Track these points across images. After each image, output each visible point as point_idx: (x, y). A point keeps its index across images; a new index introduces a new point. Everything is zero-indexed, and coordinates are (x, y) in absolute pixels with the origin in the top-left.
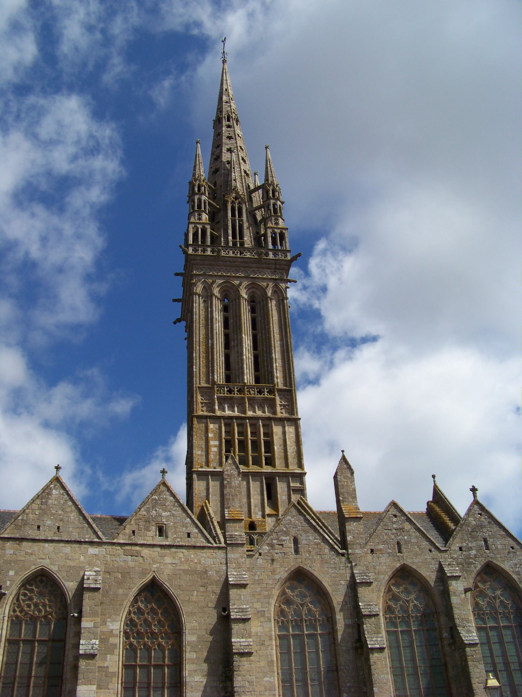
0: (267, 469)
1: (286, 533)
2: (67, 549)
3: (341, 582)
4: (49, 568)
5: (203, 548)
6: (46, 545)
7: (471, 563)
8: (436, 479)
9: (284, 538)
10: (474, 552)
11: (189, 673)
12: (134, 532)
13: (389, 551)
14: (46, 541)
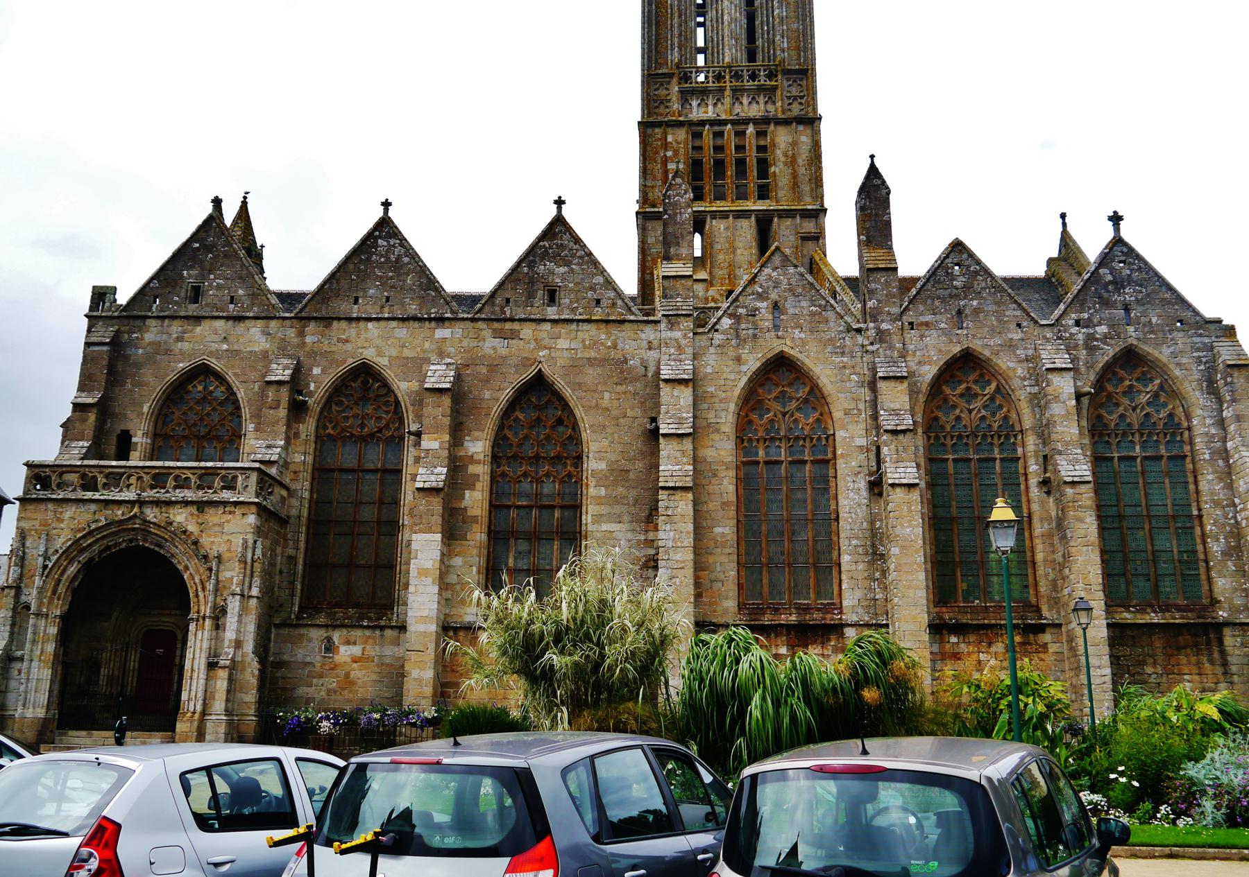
0: (761, 206)
1: (761, 297)
2: (401, 332)
4: (374, 360)
5: (623, 322)
6: (370, 325)
7: (1097, 348)
8: (1067, 220)
9: (759, 304)
10: (1103, 329)
12: (508, 301)
13: (943, 325)
14: (370, 319)
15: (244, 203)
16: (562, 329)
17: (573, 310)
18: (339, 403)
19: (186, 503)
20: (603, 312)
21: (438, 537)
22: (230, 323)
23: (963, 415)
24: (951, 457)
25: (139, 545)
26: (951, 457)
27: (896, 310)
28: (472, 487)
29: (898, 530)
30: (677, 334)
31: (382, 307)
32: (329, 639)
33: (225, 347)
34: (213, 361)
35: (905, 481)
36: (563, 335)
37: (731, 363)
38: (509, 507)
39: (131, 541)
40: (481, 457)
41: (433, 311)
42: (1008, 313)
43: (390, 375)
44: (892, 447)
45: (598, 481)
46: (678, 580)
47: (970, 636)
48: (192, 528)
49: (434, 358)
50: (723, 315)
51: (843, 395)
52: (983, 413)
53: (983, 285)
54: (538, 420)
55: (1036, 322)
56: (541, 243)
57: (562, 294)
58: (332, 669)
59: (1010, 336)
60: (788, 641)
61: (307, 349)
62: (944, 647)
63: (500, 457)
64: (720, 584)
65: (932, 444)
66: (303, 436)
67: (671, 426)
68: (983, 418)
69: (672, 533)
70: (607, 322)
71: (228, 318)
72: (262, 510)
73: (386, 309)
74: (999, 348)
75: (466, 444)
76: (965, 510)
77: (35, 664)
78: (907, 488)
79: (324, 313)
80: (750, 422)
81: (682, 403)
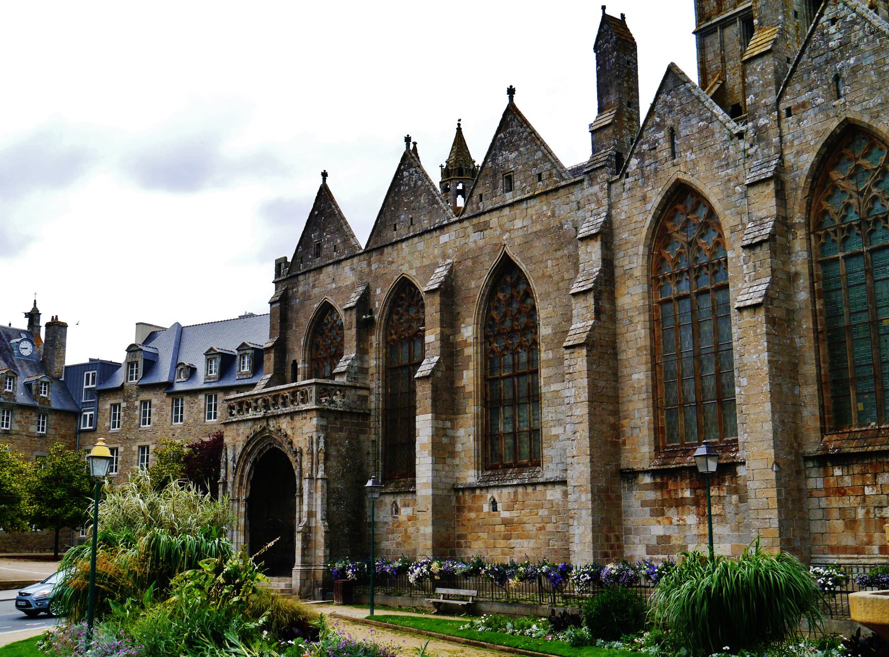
1: (659, 127)
2: (420, 244)
3: (737, 188)
5: (556, 190)
6: (404, 245)
11: (544, 381)
12: (481, 195)
13: (820, 101)
14: (402, 241)
15: (459, 130)
16: (517, 210)
17: (523, 190)
18: (398, 313)
19: (286, 415)
20: (543, 184)
21: (429, 416)
22: (335, 266)
23: (852, 201)
24: (840, 255)
25: (274, 447)
26: (840, 255)
27: (771, 99)
28: (468, 369)
29: (746, 359)
30: (596, 188)
31: (409, 228)
32: (395, 502)
33: (334, 285)
34: (329, 298)
35: (749, 303)
36: (518, 216)
37: (638, 204)
38: (497, 379)
39: (270, 444)
40: (471, 340)
41: (437, 221)
43: (416, 282)
44: (751, 263)
45: (546, 345)
46: (578, 434)
47: (855, 467)
48: (289, 432)
49: (440, 261)
50: (630, 157)
51: (728, 212)
52: (875, 191)
53: (861, 34)
54: (512, 296)
56: (499, 136)
58: (398, 527)
60: (691, 483)
61: (373, 275)
62: (828, 481)
63: (490, 336)
64: (638, 430)
65: (823, 245)
66: (374, 345)
67: (581, 284)
68: (875, 199)
69: (573, 390)
70: (546, 193)
71: (333, 263)
72: (322, 413)
73: (411, 229)
74: (879, 108)
75: (463, 330)
76: (859, 315)
77: (235, 533)
78: (752, 311)
79: (380, 245)
80: (663, 260)
81: (593, 259)
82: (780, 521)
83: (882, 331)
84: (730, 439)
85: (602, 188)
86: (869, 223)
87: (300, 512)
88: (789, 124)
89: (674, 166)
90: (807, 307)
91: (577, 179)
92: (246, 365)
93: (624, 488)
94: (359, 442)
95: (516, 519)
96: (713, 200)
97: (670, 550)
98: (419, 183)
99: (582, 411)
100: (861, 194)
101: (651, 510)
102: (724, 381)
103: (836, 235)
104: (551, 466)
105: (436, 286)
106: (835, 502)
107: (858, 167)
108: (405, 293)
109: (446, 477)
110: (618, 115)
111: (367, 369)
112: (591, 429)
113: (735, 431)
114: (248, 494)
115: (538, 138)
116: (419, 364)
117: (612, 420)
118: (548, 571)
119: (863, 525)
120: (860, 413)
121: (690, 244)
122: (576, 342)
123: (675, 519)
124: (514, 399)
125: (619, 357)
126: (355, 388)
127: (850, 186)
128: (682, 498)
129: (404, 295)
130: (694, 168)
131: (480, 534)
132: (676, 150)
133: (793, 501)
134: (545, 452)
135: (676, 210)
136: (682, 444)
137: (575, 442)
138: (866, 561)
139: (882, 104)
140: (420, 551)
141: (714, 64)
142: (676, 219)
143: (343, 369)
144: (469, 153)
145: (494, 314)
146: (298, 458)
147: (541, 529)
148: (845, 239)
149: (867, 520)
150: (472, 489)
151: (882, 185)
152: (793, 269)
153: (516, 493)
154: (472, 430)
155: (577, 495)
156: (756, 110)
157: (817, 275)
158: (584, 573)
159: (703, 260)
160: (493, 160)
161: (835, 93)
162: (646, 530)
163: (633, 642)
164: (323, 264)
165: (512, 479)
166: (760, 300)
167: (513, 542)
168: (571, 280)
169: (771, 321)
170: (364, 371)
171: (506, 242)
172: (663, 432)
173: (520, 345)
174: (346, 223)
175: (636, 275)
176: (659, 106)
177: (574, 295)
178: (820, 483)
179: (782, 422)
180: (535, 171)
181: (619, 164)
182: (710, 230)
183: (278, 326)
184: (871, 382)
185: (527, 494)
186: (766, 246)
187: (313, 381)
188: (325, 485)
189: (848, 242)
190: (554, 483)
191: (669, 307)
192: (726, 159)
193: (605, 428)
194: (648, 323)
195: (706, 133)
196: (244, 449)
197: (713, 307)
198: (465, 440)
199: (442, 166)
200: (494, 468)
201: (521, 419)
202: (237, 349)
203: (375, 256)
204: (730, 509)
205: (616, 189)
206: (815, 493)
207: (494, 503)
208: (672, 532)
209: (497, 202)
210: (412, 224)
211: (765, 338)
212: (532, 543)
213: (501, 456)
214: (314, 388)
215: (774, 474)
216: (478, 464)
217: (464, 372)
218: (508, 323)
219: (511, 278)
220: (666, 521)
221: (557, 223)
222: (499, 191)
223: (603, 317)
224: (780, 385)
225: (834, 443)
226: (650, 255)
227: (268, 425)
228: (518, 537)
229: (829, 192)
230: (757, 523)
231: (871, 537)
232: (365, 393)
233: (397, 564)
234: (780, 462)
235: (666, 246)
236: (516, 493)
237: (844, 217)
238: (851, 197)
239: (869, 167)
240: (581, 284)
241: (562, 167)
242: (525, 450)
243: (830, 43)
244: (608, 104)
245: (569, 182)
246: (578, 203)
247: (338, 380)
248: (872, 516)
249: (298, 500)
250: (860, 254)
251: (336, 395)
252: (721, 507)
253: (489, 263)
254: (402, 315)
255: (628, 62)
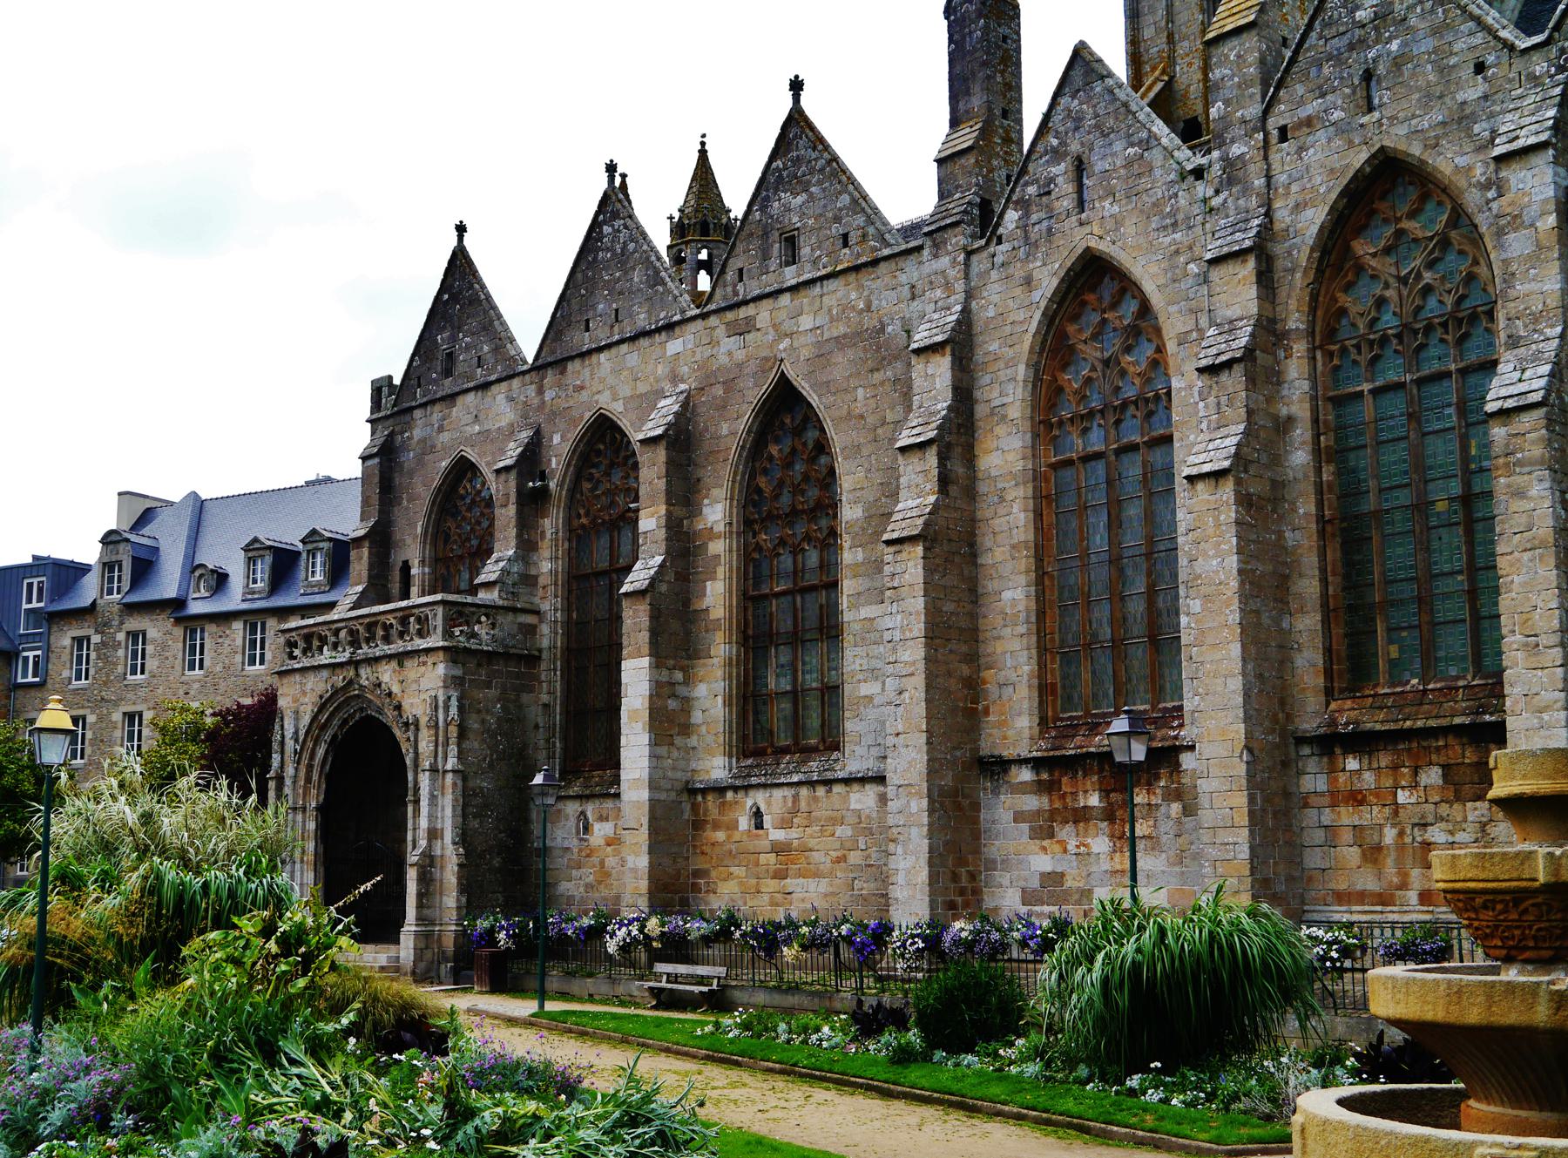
1: (1057, 155)
2: (631, 356)
5: (875, 263)
6: (603, 356)
11: (849, 602)
12: (741, 271)
13: (1337, 115)
14: (600, 349)
15: (703, 153)
16: (805, 298)
17: (815, 262)
18: (590, 478)
19: (390, 657)
21: (645, 661)
22: (480, 393)
23: (1388, 293)
26: (1366, 387)
27: (1253, 110)
28: (714, 579)
29: (1200, 566)
30: (945, 261)
31: (612, 327)
32: (583, 813)
34: (468, 450)
35: (1206, 468)
36: (806, 308)
37: (1018, 291)
38: (765, 597)
40: (720, 528)
41: (662, 316)
42: (1457, 47)
43: (625, 424)
44: (1212, 400)
45: (853, 538)
46: (906, 695)
48: (395, 689)
49: (668, 387)
50: (1006, 207)
52: (1428, 277)
54: (794, 451)
55: (1511, 48)
56: (774, 165)
57: (802, 239)
58: (588, 856)
59: (1460, 97)
60: (1101, 783)
62: (1336, 779)
63: (755, 521)
64: (1011, 689)
65: (1336, 369)
66: (548, 535)
67: (915, 431)
68: (1428, 290)
69: (899, 617)
70: (856, 269)
71: (476, 388)
72: (454, 654)
73: (616, 329)
74: (1439, 131)
75: (706, 510)
76: (1396, 493)
77: (298, 866)
78: (1213, 482)
79: (559, 356)
80: (1060, 390)
81: (938, 387)
82: (1252, 848)
83: (1434, 522)
84: (1169, 705)
85: (954, 262)
86: (1416, 332)
87: (414, 829)
88: (1282, 155)
89: (1081, 224)
90: (1306, 476)
91: (912, 244)
92: (318, 568)
93: (985, 789)
94: (520, 707)
95: (795, 843)
96: (1149, 287)
97: (1061, 898)
98: (631, 246)
99: (914, 654)
100: (1403, 281)
101: (1031, 829)
102: (1161, 605)
103: (1360, 353)
104: (859, 750)
105: (659, 431)
106: (1347, 816)
107: (1400, 233)
108: (604, 443)
109: (674, 769)
110: (985, 133)
111: (536, 577)
112: (929, 687)
113: (1178, 692)
114: (322, 797)
115: (844, 170)
116: (628, 569)
117: (965, 670)
118: (852, 934)
119: (1393, 855)
120: (1393, 664)
121: (1106, 363)
122: (905, 534)
123: (1072, 845)
124: (795, 633)
125: (980, 561)
126: (514, 610)
127: (1385, 266)
128: (1085, 807)
129: (602, 447)
130: (1117, 229)
131: (732, 869)
132: (1086, 196)
133: (1275, 814)
134: (849, 726)
135: (1084, 304)
136: (1087, 714)
137: (901, 708)
138: (1396, 917)
139: (1444, 124)
140: (627, 899)
141: (1155, 46)
142: (1084, 319)
143: (493, 577)
144: (719, 195)
145: (762, 482)
146: (411, 734)
147: (838, 860)
148: (1375, 360)
149: (1400, 847)
150: (720, 790)
151: (1441, 266)
152: (1284, 411)
153: (796, 798)
154: (720, 686)
155: (903, 801)
156: (1226, 129)
157: (1325, 421)
158: (913, 936)
159: (1130, 392)
160: (763, 209)
161: (1363, 102)
162: (1020, 862)
163: (996, 1055)
164: (457, 389)
165: (790, 773)
166: (1226, 464)
167: (790, 883)
168: (898, 424)
169: (1244, 500)
170: (529, 580)
171: (784, 355)
172: (1054, 693)
173: (808, 538)
174: (499, 316)
175: (1011, 417)
176: (1057, 119)
177: (903, 450)
178: (1321, 784)
179: (1260, 676)
180: (837, 230)
181: (985, 220)
182: (1143, 339)
183: (375, 499)
184: (1414, 608)
185: (816, 799)
186: (1238, 370)
187: (438, 597)
188: (460, 783)
189: (1380, 365)
190: (863, 780)
191: (1068, 473)
192: (1173, 214)
193: (954, 685)
194: (1031, 501)
195: (1138, 168)
196: (314, 719)
197: (1145, 475)
198: (707, 704)
199: (671, 218)
200: (759, 753)
201: (808, 667)
202: (303, 541)
203: (550, 377)
204: (1167, 827)
205: (979, 263)
206: (1313, 800)
207: (758, 815)
208: (1068, 866)
209: (770, 282)
210: (617, 321)
211: (1233, 530)
212: (823, 886)
213: (771, 732)
214: (440, 610)
215: (1244, 767)
216: (730, 746)
217: (708, 583)
218: (786, 499)
219: (793, 419)
220: (1057, 848)
221: (875, 322)
222: (773, 264)
223: (954, 490)
224: (1257, 612)
225: (1347, 714)
226: (1037, 381)
227: (358, 675)
228: (800, 875)
229: (1350, 277)
230: (1213, 852)
231: (1404, 876)
232: (530, 619)
233: (586, 922)
234: (1255, 745)
235: (1064, 367)
236: (796, 798)
237: (1375, 320)
238: (1387, 286)
239: (1420, 234)
240: (915, 431)
241: (886, 223)
242: (814, 721)
243: (1358, 14)
244: (967, 112)
245: (896, 249)
246: (913, 287)
247: (484, 596)
248: (1408, 840)
249: (410, 809)
250: (1400, 386)
251: (480, 623)
252: (1151, 823)
253: (754, 392)
254: (598, 481)
255: (1005, 38)
